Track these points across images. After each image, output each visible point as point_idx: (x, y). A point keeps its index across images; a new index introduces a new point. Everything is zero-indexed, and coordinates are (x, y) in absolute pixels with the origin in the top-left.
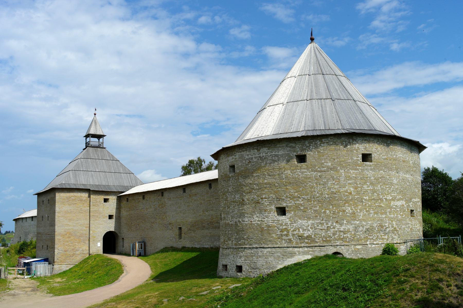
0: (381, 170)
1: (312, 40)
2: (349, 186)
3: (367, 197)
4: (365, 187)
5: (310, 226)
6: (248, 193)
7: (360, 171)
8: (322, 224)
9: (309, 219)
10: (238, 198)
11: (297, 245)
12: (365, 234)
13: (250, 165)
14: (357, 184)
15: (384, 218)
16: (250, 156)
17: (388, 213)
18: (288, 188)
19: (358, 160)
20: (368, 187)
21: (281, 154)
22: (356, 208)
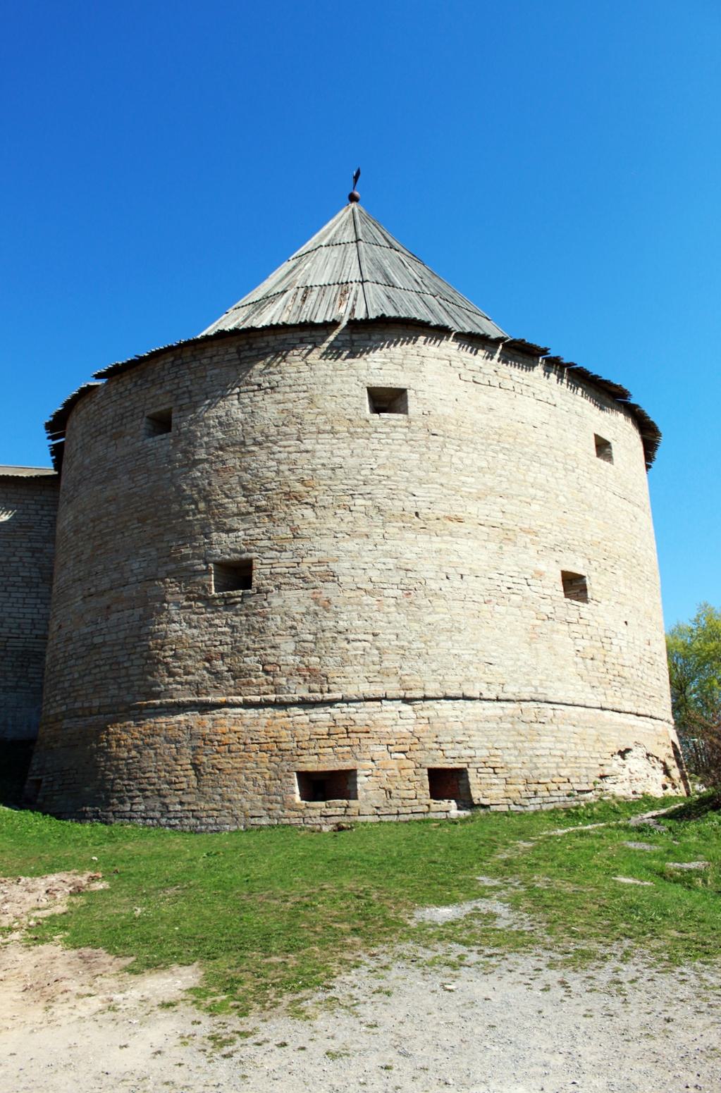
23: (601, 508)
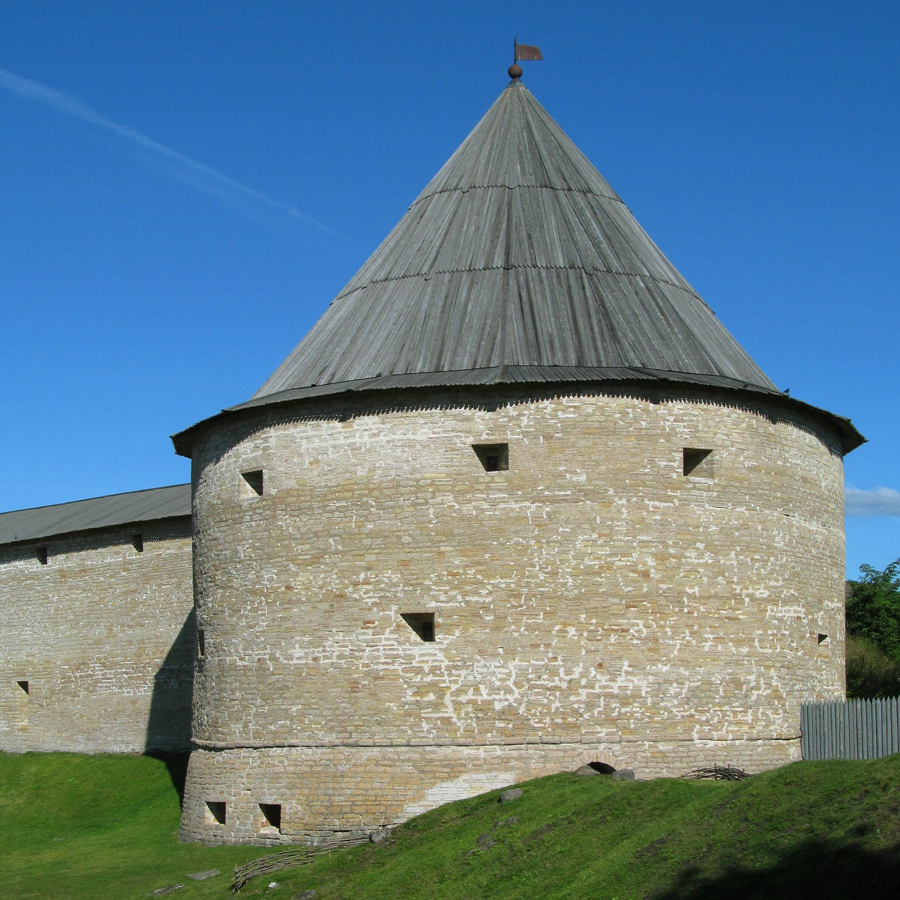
0: (740, 503)
1: (514, 76)
2: (641, 552)
3: (697, 589)
4: (691, 554)
5: (514, 676)
6: (306, 563)
7: (677, 504)
8: (554, 672)
9: (511, 653)
10: (271, 580)
11: (470, 740)
12: (686, 707)
13: (315, 473)
14: (667, 546)
15: (746, 656)
16: (317, 443)
17: (756, 640)
18: (443, 553)
19: (672, 469)
20: (700, 555)
21: (424, 438)
22: (662, 623)
23: (469, 532)
